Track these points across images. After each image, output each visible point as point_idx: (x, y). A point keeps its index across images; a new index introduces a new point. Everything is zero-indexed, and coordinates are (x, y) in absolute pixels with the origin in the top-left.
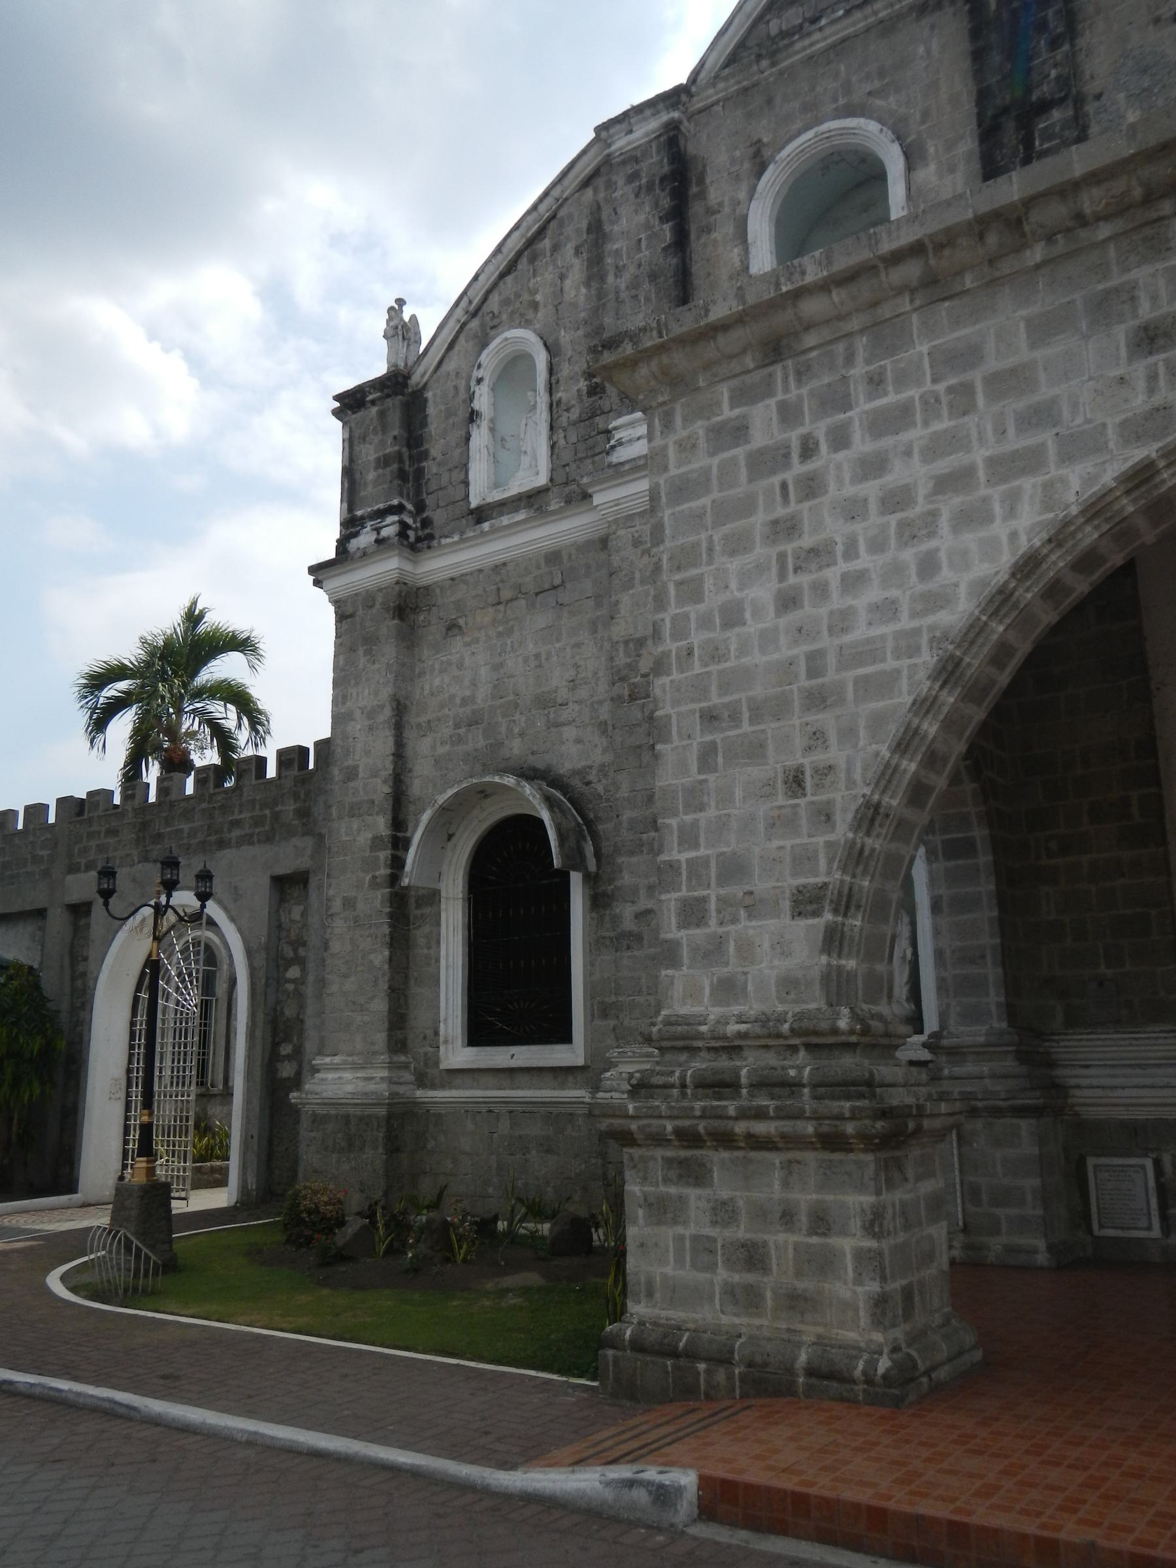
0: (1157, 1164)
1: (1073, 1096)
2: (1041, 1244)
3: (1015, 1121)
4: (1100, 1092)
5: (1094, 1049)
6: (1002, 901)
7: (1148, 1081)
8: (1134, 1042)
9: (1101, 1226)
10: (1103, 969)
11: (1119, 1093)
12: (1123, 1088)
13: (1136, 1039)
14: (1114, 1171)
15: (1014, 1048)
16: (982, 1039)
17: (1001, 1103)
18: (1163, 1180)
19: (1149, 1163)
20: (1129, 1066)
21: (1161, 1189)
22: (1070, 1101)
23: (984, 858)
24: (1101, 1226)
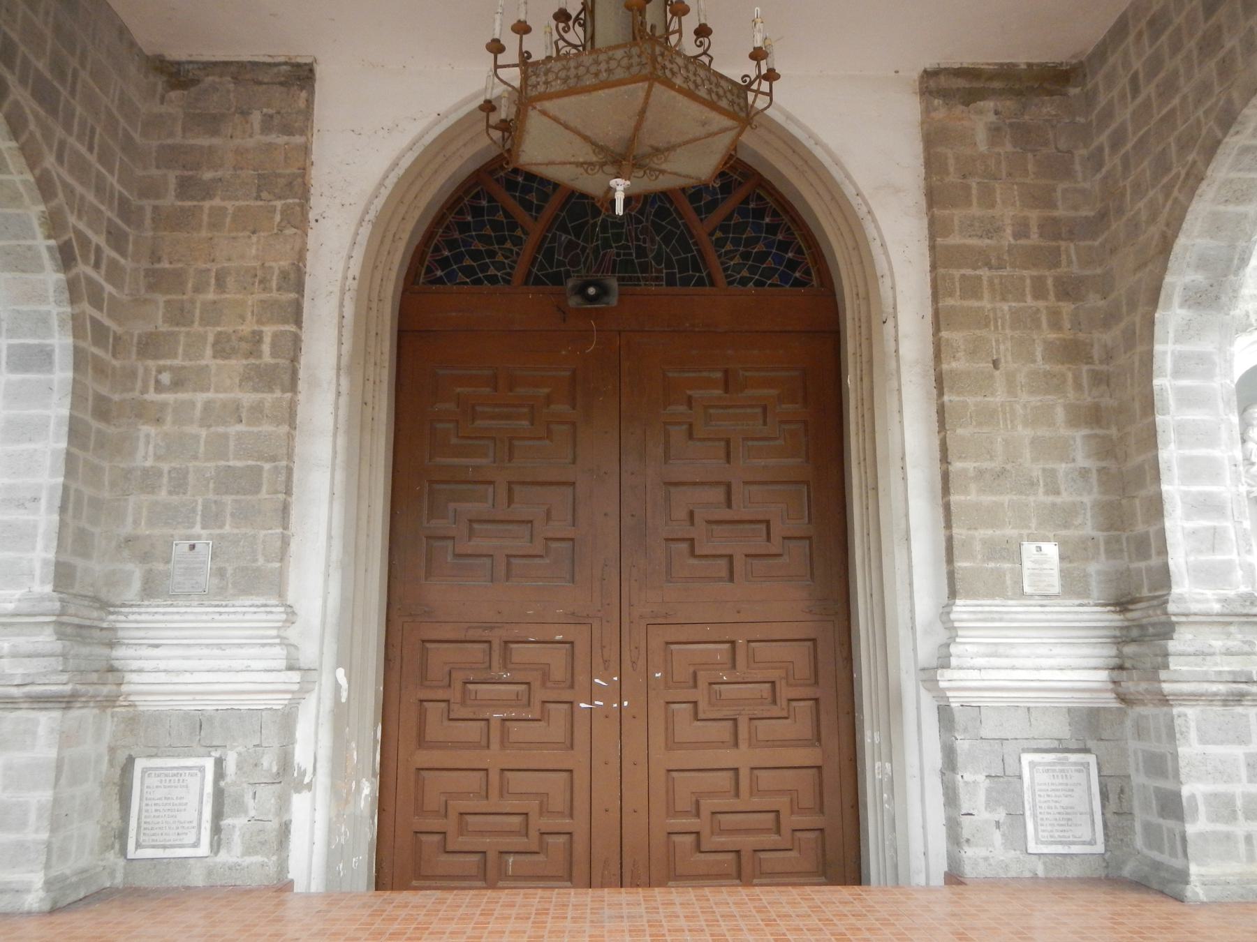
0: (219, 763)
1: (129, 683)
2: (37, 879)
3: (33, 714)
4: (162, 677)
5: (169, 625)
6: (76, 432)
7: (225, 664)
8: (217, 617)
9: (138, 846)
10: (197, 529)
11: (187, 678)
12: (192, 672)
13: (220, 613)
14: (166, 775)
15: (53, 618)
16: (10, 607)
17: (15, 691)
18: (222, 784)
19: (209, 764)
20: (207, 645)
21: (219, 794)
22: (124, 688)
23: (62, 374)
24: (138, 846)
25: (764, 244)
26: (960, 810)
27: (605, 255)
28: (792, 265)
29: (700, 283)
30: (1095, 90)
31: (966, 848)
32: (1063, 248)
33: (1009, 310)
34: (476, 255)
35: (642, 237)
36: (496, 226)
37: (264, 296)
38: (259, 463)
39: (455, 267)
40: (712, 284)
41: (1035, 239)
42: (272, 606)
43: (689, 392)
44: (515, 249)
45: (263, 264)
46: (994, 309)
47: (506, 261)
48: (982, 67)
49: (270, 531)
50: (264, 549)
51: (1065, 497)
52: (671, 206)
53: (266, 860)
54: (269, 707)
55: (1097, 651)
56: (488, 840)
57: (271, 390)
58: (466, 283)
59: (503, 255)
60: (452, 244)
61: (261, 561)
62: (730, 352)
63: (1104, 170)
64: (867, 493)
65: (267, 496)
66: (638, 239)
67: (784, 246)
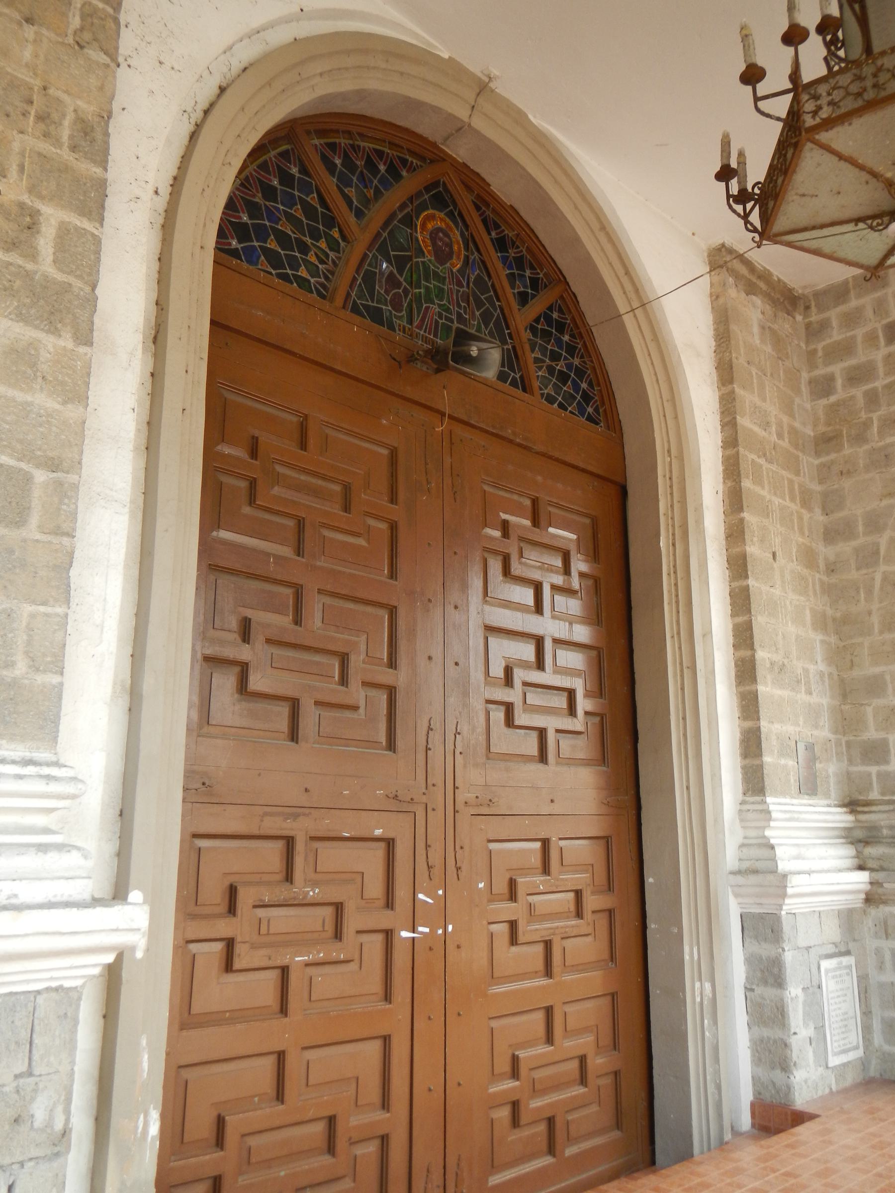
26: (789, 1030)
27: (427, 308)
29: (514, 384)
30: (824, 325)
31: (795, 1072)
32: (800, 459)
33: (779, 506)
34: (283, 239)
35: (463, 304)
36: (309, 210)
37: (44, 147)
38: (23, 465)
39: (256, 244)
41: (785, 444)
43: (504, 516)
44: (332, 255)
45: (45, 88)
46: (770, 501)
47: (320, 266)
48: (756, 264)
49: (42, 609)
50: (29, 643)
51: (815, 699)
52: (490, 281)
54: (54, 984)
55: (833, 852)
56: (282, 1173)
57: (56, 332)
58: (271, 273)
59: (316, 254)
60: (253, 209)
61: (21, 668)
62: (539, 478)
63: (833, 399)
64: (682, 671)
65: (38, 536)
66: (459, 306)
67: (580, 373)
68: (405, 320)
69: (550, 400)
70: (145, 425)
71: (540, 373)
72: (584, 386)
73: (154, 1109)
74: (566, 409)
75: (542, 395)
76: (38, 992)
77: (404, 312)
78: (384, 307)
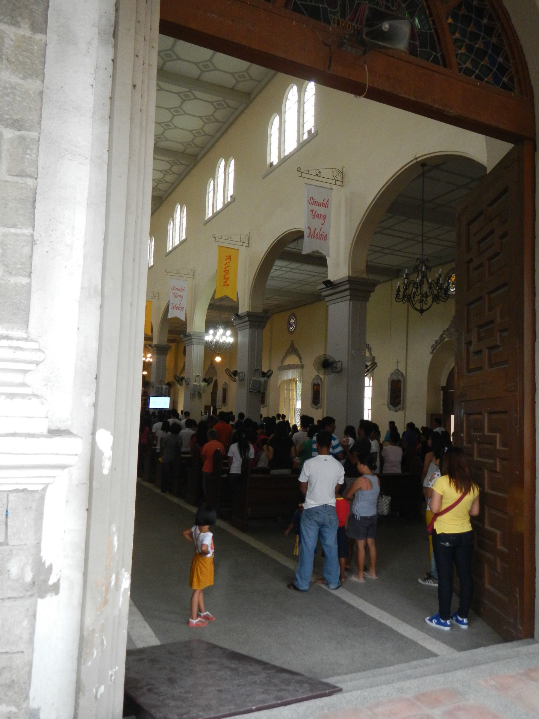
25: (483, 43)
27: (359, 4)
28: (502, 69)
29: (435, 61)
40: (445, 66)
42: (18, 339)
49: (13, 230)
53: (14, 709)
54: (21, 487)
57: (16, 24)
68: (339, 15)
69: (468, 72)
70: (108, 100)
71: (460, 52)
72: (500, 60)
73: (126, 571)
74: (482, 80)
75: (460, 70)
76: (10, 491)
77: (338, 8)
78: (321, 6)
